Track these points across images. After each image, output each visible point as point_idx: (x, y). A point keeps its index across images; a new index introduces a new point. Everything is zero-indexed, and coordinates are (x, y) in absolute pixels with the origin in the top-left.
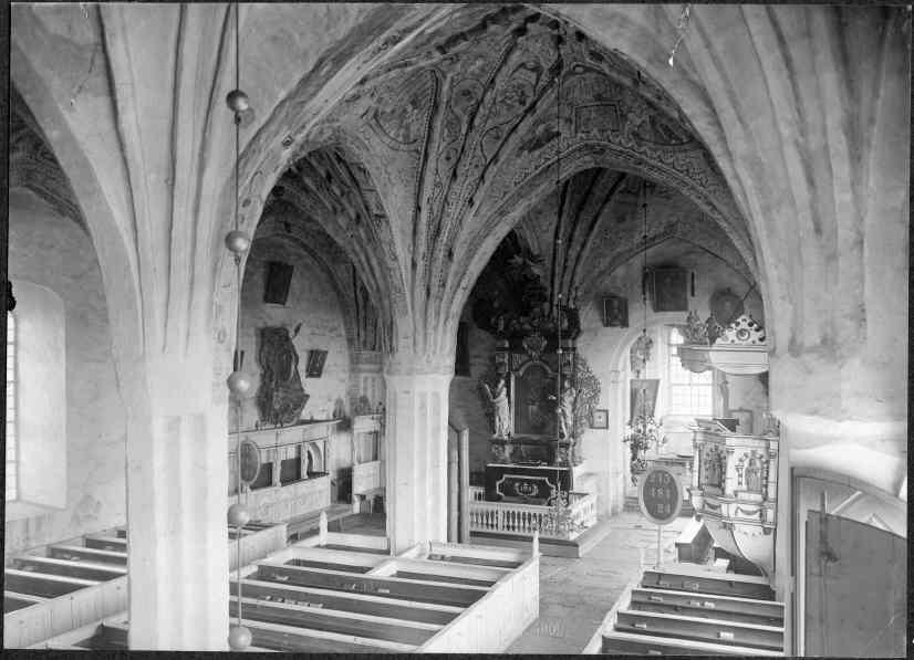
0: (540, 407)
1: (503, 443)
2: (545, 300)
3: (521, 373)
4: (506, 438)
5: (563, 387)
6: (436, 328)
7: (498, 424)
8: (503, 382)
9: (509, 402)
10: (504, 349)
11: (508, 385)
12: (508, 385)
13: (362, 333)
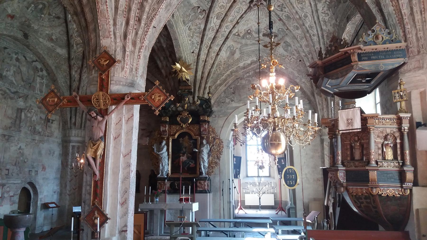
0: (188, 158)
1: (165, 179)
2: (190, 93)
3: (176, 136)
4: (166, 176)
5: (202, 143)
6: (133, 52)
8: (164, 142)
9: (168, 155)
10: (166, 122)
13: (73, 117)
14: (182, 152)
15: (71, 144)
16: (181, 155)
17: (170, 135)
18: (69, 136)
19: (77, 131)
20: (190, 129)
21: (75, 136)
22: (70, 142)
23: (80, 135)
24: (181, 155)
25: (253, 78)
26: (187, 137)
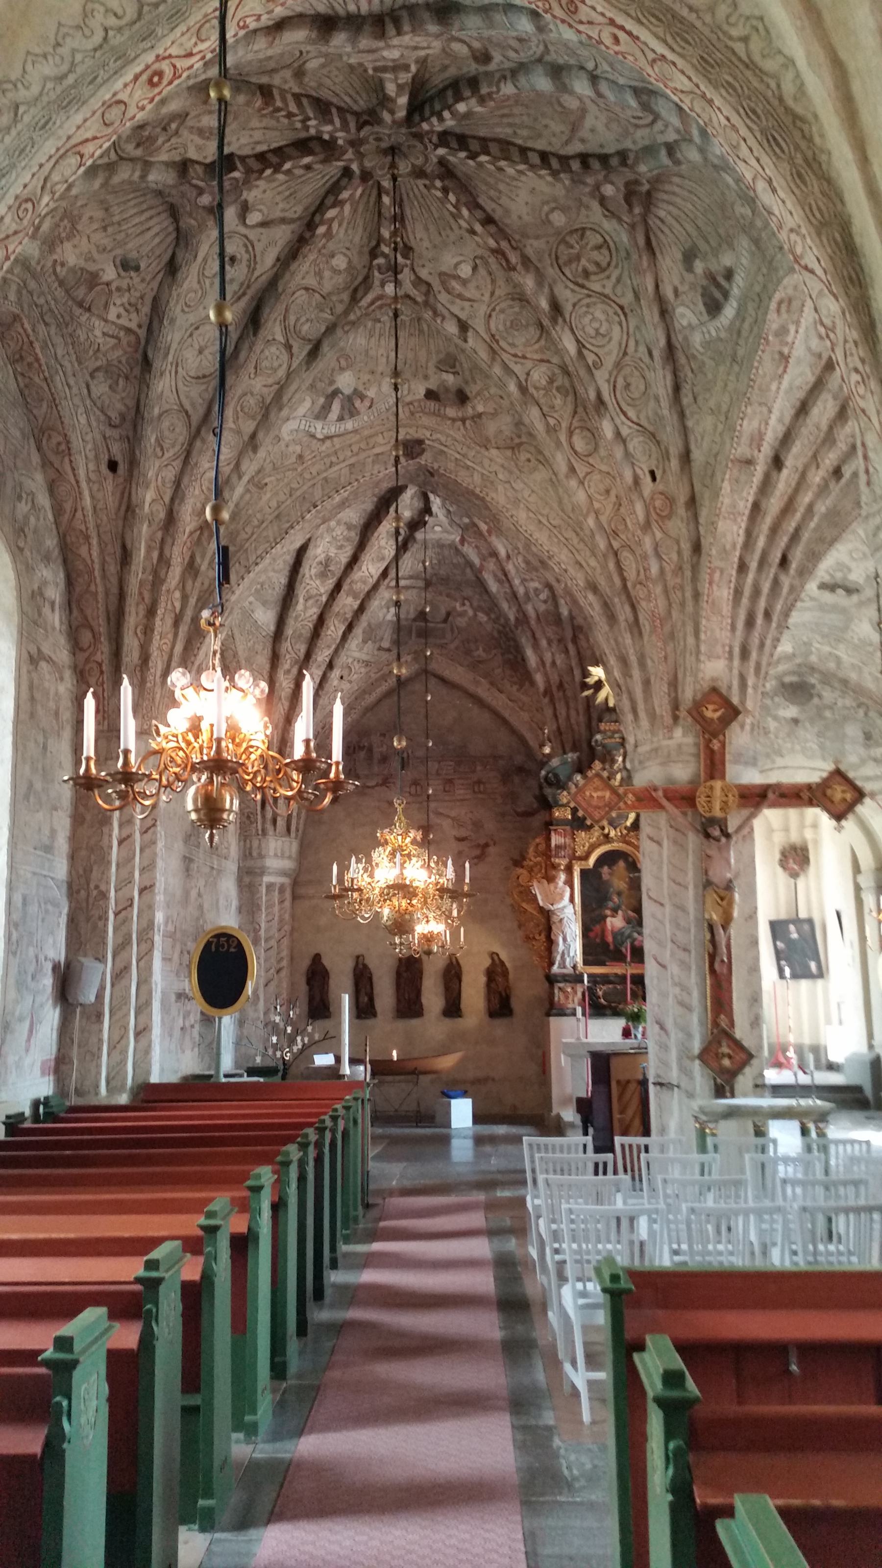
7: (561, 947)
11: (570, 883)
12: (570, 883)
14: (610, 904)
15: (266, 879)
16: (608, 912)
17: (574, 857)
18: (261, 856)
19: (280, 843)
20: (628, 843)
21: (276, 855)
22: (263, 872)
23: (287, 854)
24: (608, 912)
25: (777, 699)
26: (621, 864)
